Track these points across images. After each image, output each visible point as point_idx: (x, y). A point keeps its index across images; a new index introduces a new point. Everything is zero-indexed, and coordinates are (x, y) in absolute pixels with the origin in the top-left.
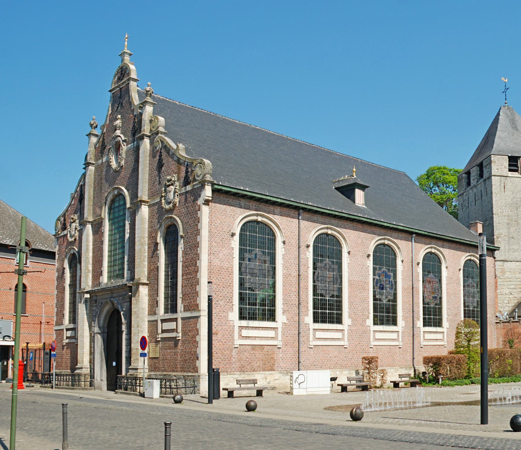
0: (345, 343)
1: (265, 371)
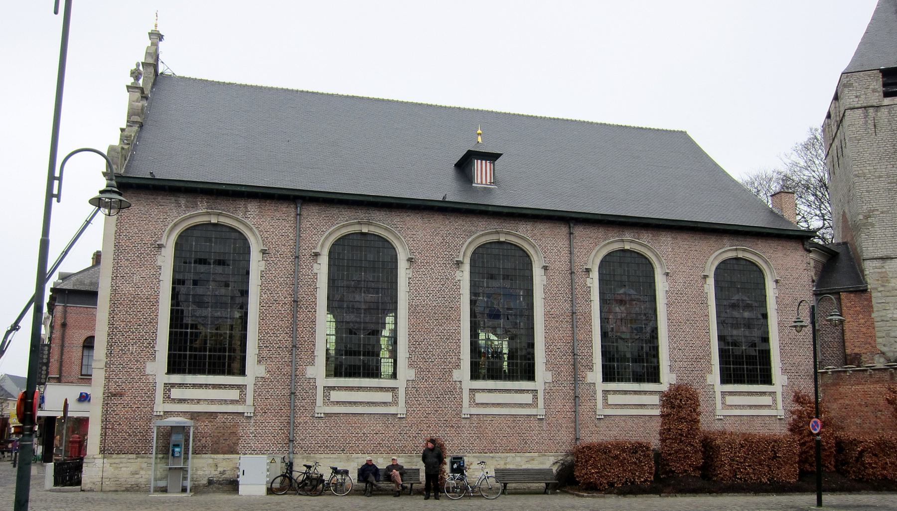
0: (400, 409)
1: (218, 453)
